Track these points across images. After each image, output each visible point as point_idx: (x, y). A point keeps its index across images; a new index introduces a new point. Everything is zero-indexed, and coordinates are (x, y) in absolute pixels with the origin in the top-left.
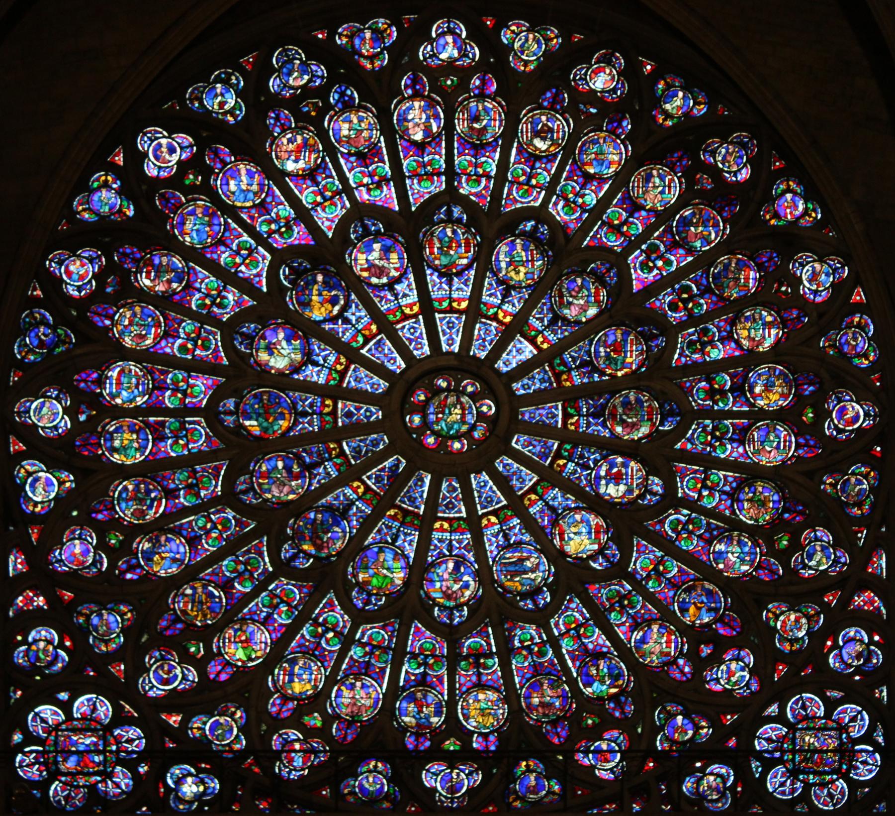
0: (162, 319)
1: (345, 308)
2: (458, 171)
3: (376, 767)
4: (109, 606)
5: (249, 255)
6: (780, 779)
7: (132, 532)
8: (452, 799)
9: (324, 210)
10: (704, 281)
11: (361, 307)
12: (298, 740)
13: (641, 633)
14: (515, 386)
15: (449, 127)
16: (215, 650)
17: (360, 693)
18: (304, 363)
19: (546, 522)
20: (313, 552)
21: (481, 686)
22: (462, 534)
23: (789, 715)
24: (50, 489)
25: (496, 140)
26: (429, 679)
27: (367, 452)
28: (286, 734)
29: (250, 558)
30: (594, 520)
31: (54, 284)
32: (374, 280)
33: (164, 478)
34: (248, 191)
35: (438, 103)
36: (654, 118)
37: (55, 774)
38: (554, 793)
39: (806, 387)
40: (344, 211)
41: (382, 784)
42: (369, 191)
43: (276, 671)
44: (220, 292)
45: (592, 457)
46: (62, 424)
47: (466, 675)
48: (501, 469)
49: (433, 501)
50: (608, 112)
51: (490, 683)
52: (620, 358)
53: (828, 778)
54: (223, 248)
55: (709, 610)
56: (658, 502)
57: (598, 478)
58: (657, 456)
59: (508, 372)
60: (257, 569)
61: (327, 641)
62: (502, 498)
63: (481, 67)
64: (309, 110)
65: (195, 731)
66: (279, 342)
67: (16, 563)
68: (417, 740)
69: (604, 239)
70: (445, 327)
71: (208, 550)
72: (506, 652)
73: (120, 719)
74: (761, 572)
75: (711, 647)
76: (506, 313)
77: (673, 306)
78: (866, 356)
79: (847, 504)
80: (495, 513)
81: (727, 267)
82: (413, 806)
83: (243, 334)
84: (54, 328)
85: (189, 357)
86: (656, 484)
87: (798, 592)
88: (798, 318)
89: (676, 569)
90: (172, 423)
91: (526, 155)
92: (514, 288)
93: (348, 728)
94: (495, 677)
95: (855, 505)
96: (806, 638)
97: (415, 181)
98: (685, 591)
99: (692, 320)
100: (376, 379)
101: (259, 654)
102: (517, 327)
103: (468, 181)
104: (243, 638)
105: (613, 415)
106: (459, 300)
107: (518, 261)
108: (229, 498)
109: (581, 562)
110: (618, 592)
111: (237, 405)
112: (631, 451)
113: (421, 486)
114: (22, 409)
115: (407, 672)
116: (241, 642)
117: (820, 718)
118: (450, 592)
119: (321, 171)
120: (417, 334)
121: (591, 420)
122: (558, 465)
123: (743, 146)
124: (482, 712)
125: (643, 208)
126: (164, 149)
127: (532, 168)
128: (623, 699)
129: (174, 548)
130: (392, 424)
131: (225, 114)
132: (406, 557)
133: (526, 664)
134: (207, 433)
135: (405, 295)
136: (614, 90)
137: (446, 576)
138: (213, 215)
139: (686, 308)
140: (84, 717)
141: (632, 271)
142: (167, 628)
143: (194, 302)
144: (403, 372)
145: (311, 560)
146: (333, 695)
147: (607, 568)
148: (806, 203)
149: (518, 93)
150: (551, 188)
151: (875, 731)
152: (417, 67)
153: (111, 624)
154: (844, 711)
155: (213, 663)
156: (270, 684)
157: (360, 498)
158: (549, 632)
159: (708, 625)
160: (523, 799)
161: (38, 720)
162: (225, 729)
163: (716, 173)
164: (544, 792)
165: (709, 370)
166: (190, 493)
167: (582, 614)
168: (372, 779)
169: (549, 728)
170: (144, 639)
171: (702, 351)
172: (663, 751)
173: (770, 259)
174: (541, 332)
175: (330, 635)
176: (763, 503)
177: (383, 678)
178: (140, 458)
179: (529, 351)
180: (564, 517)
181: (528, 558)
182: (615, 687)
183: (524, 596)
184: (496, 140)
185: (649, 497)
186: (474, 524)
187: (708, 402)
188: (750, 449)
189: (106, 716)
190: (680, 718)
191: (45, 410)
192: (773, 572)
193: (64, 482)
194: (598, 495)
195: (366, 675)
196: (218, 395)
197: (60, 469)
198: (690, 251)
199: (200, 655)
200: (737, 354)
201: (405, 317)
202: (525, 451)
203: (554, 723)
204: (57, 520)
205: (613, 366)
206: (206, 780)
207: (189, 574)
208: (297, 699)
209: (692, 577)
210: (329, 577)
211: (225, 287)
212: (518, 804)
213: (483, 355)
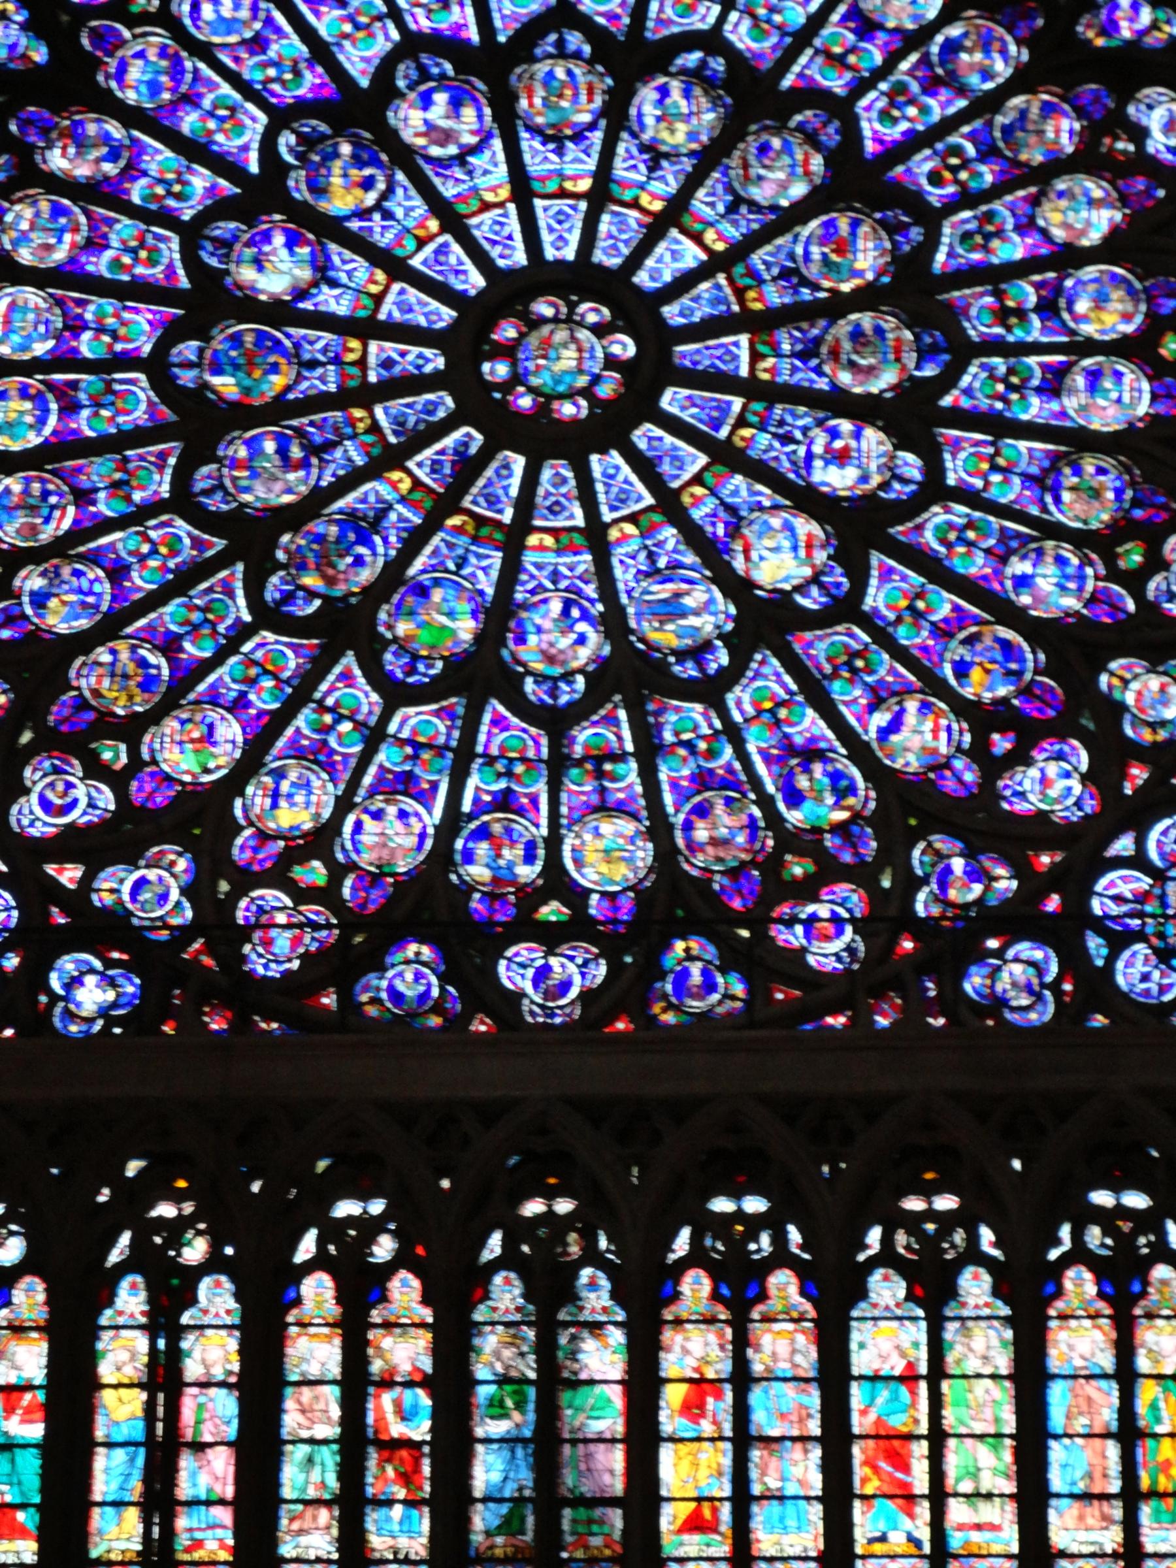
0: (83, 219)
6: (1140, 968)
9: (354, 42)
11: (412, 192)
12: (284, 908)
13: (887, 717)
16: (146, 756)
18: (315, 284)
19: (720, 530)
21: (605, 807)
22: (576, 553)
28: (262, 898)
29: (213, 601)
30: (805, 526)
32: (435, 151)
34: (235, 20)
38: (733, 998)
39: (1162, 301)
41: (429, 985)
43: (250, 790)
49: (525, 503)
55: (1009, 673)
57: (810, 456)
58: (911, 417)
59: (658, 290)
60: (222, 619)
65: (104, 895)
66: (274, 252)
69: (818, 77)
71: (140, 589)
72: (649, 751)
75: (1012, 735)
76: (655, 196)
77: (935, 178)
80: (633, 518)
82: (482, 1023)
83: (214, 240)
85: (126, 278)
86: (911, 464)
92: (666, 156)
98: (964, 642)
100: (434, 304)
101: (222, 761)
104: (196, 735)
105: (835, 353)
107: (675, 115)
108: (182, 501)
109: (782, 599)
110: (846, 646)
111: (201, 351)
112: (865, 410)
113: (510, 476)
115: (477, 789)
116: (192, 741)
118: (553, 651)
120: (505, 233)
122: (743, 439)
124: (608, 858)
125: (881, 27)
128: (855, 829)
129: (85, 585)
130: (461, 377)
132: (481, 593)
135: (486, 172)
137: (547, 624)
139: (956, 181)
141: (865, 125)
143: (136, 193)
144: (481, 293)
145: (317, 603)
147: (826, 606)
156: (238, 812)
157: (403, 500)
158: (724, 714)
159: (1005, 701)
160: (678, 1009)
162: (155, 888)
165: (997, 277)
167: (784, 686)
169: (726, 881)
170: (26, 737)
171: (986, 248)
172: (929, 918)
174: (711, 225)
175: (346, 727)
176: (1096, 493)
178: (34, 440)
179: (692, 255)
180: (751, 523)
181: (688, 593)
183: (681, 655)
186: (596, 537)
187: (998, 330)
192: (1116, 607)
195: (406, 793)
199: (118, 766)
200: (1044, 251)
201: (486, 207)
202: (685, 416)
203: (732, 873)
206: (120, 981)
207: (109, 628)
212: (670, 1018)
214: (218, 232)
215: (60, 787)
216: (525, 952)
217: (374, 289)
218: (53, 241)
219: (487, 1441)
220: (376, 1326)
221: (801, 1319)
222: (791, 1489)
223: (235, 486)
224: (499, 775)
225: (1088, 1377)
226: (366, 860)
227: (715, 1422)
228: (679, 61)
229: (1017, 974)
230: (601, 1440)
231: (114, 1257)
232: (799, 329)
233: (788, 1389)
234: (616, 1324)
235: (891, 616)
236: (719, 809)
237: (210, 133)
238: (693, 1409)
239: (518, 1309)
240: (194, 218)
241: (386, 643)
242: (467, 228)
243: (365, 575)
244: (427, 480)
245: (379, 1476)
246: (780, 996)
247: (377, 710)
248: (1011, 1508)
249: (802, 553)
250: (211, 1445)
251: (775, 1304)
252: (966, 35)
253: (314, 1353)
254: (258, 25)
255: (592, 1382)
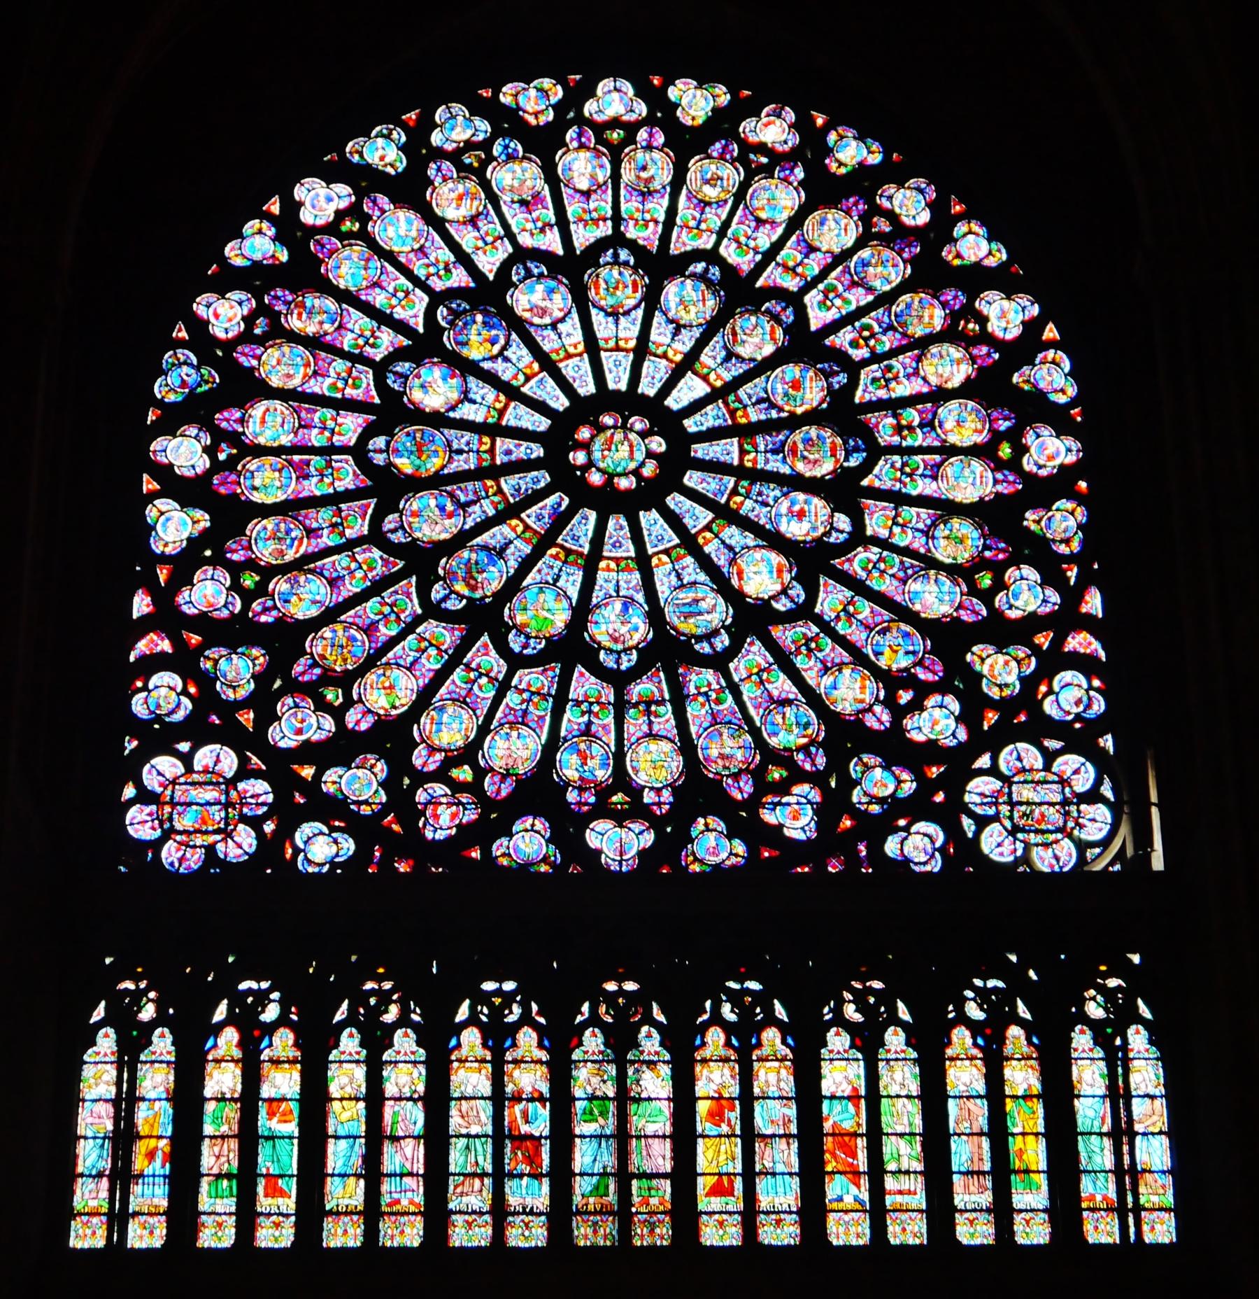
0: (311, 359)
1: (504, 348)
2: (625, 216)
3: (533, 825)
4: (240, 650)
5: (406, 296)
7: (268, 572)
8: (620, 863)
9: (485, 253)
10: (886, 319)
11: (522, 345)
12: (446, 795)
13: (832, 678)
14: (686, 422)
15: (616, 177)
16: (355, 697)
17: (516, 743)
18: (461, 402)
20: (466, 592)
21: (651, 735)
23: (1003, 767)
24: (181, 528)
25: (664, 187)
26: (594, 728)
27: (527, 490)
30: (775, 558)
31: (199, 327)
32: (536, 320)
33: (306, 517)
35: (604, 154)
36: (826, 168)
37: (168, 834)
38: (737, 855)
40: (506, 255)
42: (532, 235)
43: (423, 720)
44: (373, 332)
45: (772, 494)
46: (201, 463)
47: (635, 723)
48: (672, 506)
50: (778, 160)
51: (663, 733)
52: (800, 394)
53: (1051, 837)
54: (378, 290)
55: (907, 653)
56: (846, 540)
58: (844, 491)
60: (403, 611)
61: (480, 688)
62: (674, 536)
63: (649, 121)
64: (472, 164)
65: (329, 785)
66: (435, 381)
67: (141, 605)
68: (580, 795)
69: (779, 281)
70: (611, 365)
72: (679, 701)
73: (244, 772)
74: (962, 612)
76: (676, 352)
77: (854, 344)
78: (1063, 391)
79: (1054, 541)
81: (909, 306)
82: (575, 868)
83: (395, 373)
84: (198, 368)
85: (339, 396)
86: (843, 522)
87: (1002, 632)
88: (989, 354)
89: (868, 610)
90: (317, 461)
91: (695, 201)
92: (685, 326)
93: (503, 780)
94: (668, 726)
95: (1061, 541)
96: (1017, 683)
97: (581, 225)
98: (879, 633)
99: (876, 358)
100: (537, 416)
101: (404, 701)
102: (688, 364)
103: (636, 225)
104: (387, 684)
105: (794, 450)
106: (627, 340)
107: (688, 300)
108: (376, 537)
109: (764, 606)
110: (804, 635)
111: (388, 443)
114: (159, 448)
115: (569, 721)
116: (384, 688)
117: (1038, 771)
118: (617, 635)
119: (482, 217)
121: (769, 455)
123: (921, 191)
124: (655, 766)
125: (819, 250)
126: (322, 199)
127: (702, 212)
128: (813, 750)
131: (385, 166)
133: (703, 712)
134: (354, 472)
135: (569, 335)
136: (785, 142)
138: (367, 260)
139: (867, 345)
140: (206, 771)
141: (809, 310)
142: (303, 674)
144: (566, 410)
145: (464, 601)
146: (486, 746)
147: (790, 610)
148: (989, 240)
149: (687, 145)
150: (722, 233)
151: (1102, 784)
152: (582, 121)
153: (237, 671)
154: (1066, 763)
155: (352, 710)
157: (518, 537)
158: (727, 675)
159: (907, 669)
161: (155, 773)
162: (361, 783)
163: (892, 216)
164: (724, 855)
165: (894, 406)
166: (332, 532)
168: (528, 842)
169: (730, 781)
170: (278, 684)
171: (886, 386)
173: (955, 297)
175: (484, 680)
176: (962, 542)
177: (541, 728)
178: (281, 497)
179: (701, 389)
182: (804, 736)
183: (699, 639)
184: (664, 187)
185: (834, 534)
186: (643, 562)
188: (943, 485)
189: (230, 768)
190: (878, 771)
191: (182, 449)
192: (977, 613)
193: (198, 521)
194: (778, 533)
195: (523, 723)
196: (368, 433)
197: (195, 505)
198: (870, 290)
199: (336, 704)
200: (925, 390)
201: (569, 356)
203: (736, 777)
204: (186, 564)
205: (791, 402)
206: (340, 840)
207: (330, 616)
208: (445, 751)
209: (886, 618)
210: (485, 619)
211: (379, 328)
212: (696, 868)
213: (651, 392)
214: (398, 369)
215: (300, 716)
216: (602, 825)
217: (498, 406)
218: (292, 372)
219: (582, 1137)
220: (509, 1062)
221: (784, 1059)
222: (780, 1168)
223: (411, 528)
224: (583, 713)
225: (968, 1098)
226: (498, 764)
227: (729, 1124)
228: (691, 268)
229: (918, 845)
230: (654, 1136)
231: (339, 1017)
232: (771, 436)
233: (777, 1103)
234: (664, 1062)
235: (833, 615)
236: (725, 736)
237: (393, 307)
238: (716, 1116)
239: (601, 1052)
240: (383, 360)
241: (509, 629)
242: (559, 370)
243: (495, 585)
244: (535, 527)
245: (514, 1160)
246: (766, 854)
247: (504, 669)
248: (920, 1179)
249: (775, 574)
250: (404, 1138)
251: (766, 1051)
252: (873, 255)
253: (470, 1080)
254: (423, 241)
255: (649, 1099)
